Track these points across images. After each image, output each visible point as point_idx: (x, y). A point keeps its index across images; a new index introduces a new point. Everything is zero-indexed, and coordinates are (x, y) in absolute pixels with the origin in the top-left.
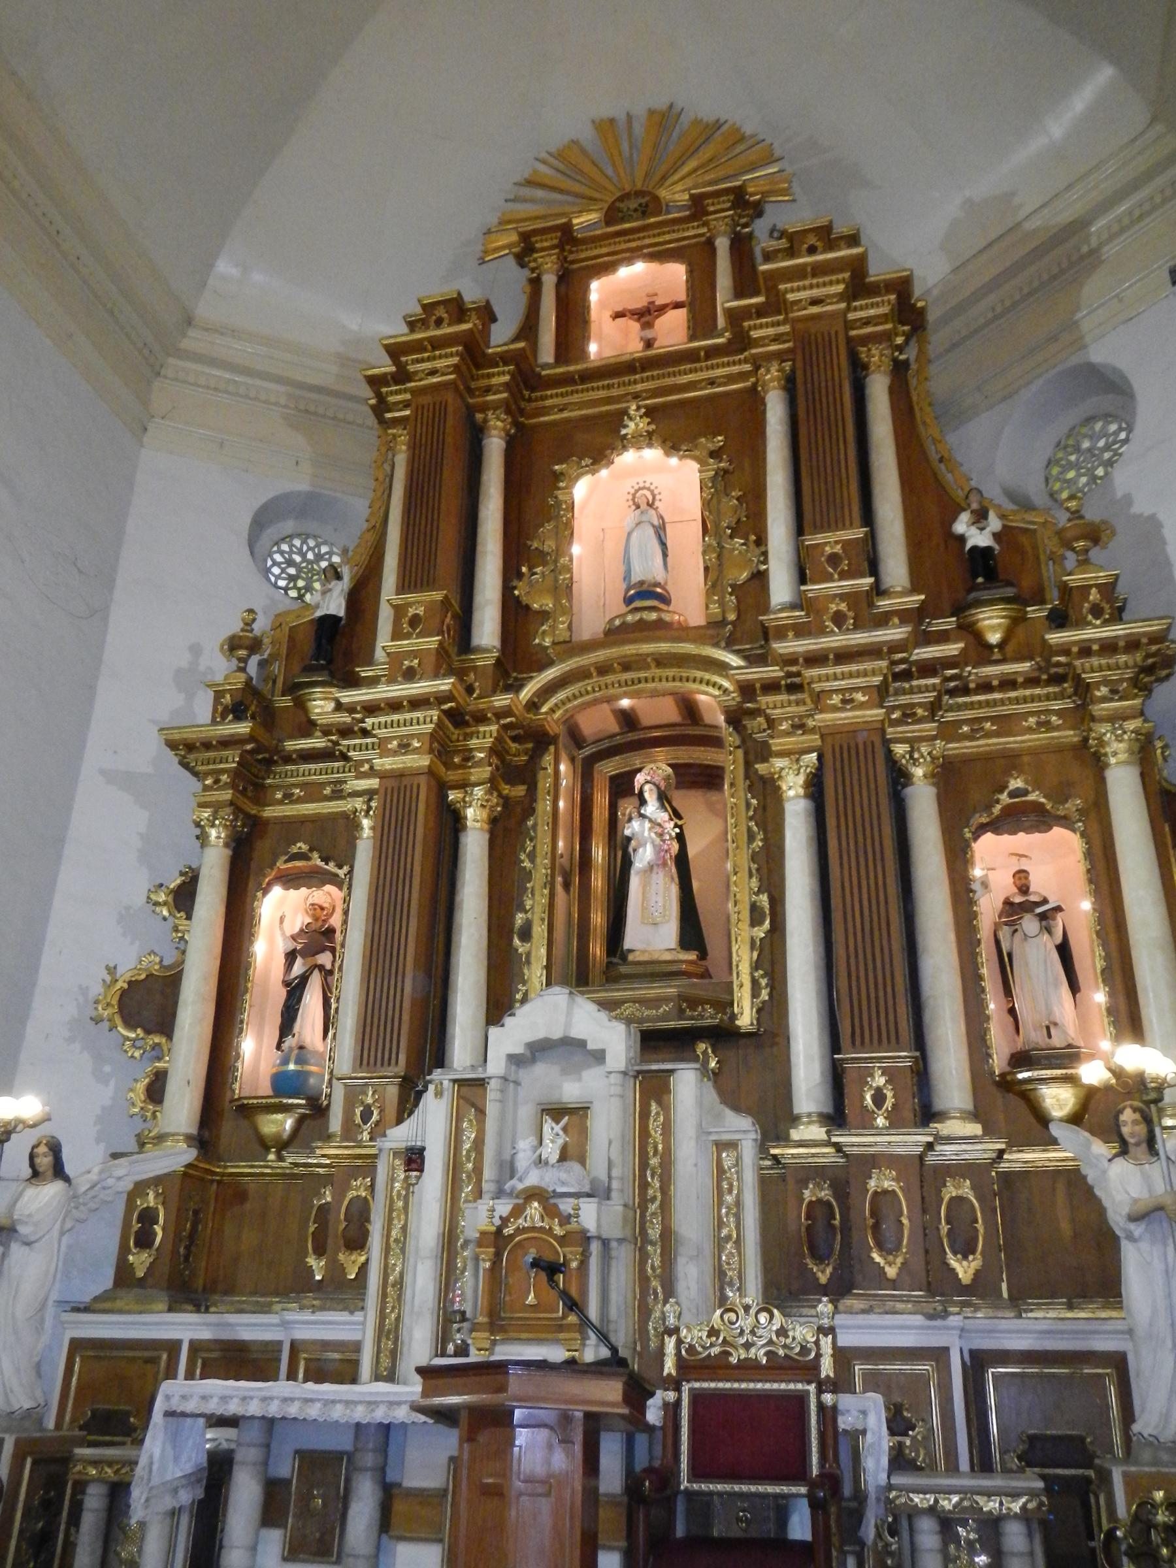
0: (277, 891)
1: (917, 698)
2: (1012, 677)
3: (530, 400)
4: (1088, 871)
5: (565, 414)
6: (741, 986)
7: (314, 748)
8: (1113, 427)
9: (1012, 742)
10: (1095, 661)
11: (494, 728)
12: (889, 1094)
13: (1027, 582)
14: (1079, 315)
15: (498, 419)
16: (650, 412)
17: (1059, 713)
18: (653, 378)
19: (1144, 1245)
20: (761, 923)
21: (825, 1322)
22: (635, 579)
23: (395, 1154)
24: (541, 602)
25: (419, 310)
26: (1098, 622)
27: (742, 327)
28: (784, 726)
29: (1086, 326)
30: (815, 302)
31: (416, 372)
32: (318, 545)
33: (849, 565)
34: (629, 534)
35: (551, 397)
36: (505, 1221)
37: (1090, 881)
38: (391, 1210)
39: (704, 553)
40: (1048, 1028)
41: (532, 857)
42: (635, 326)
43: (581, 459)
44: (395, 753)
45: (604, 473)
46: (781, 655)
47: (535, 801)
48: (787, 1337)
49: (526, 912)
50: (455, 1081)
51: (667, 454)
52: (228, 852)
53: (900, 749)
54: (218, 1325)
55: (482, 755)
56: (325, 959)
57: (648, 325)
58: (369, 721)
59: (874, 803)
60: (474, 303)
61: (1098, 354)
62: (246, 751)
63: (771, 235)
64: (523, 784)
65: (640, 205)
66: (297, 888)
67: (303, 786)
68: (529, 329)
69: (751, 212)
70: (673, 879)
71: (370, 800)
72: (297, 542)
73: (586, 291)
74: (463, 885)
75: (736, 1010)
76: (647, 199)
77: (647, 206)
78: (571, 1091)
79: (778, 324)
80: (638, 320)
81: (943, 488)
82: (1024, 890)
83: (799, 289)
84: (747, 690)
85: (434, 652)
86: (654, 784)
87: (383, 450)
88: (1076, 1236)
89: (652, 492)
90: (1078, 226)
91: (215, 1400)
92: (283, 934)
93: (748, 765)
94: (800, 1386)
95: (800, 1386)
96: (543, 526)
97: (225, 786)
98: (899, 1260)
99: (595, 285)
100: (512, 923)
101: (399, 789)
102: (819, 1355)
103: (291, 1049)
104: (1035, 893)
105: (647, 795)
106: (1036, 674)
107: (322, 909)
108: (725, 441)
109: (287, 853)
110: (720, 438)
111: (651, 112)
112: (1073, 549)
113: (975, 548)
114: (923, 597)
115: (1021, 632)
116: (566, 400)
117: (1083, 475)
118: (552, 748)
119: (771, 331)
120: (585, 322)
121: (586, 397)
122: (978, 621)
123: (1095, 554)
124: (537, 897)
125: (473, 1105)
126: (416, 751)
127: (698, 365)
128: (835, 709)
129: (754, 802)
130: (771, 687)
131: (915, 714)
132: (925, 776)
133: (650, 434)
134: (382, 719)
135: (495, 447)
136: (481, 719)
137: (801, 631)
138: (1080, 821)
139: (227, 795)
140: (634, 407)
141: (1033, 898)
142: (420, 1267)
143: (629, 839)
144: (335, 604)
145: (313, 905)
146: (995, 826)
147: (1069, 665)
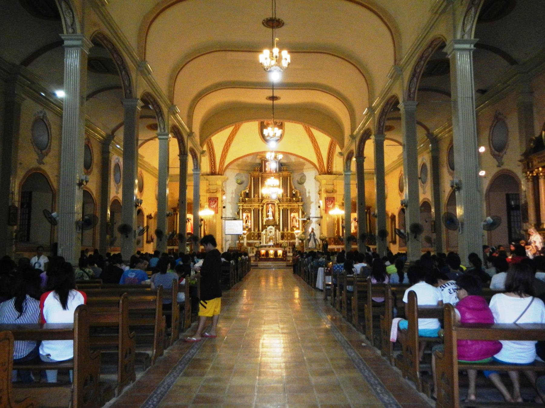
78: (271, 230)
144: (247, 192)
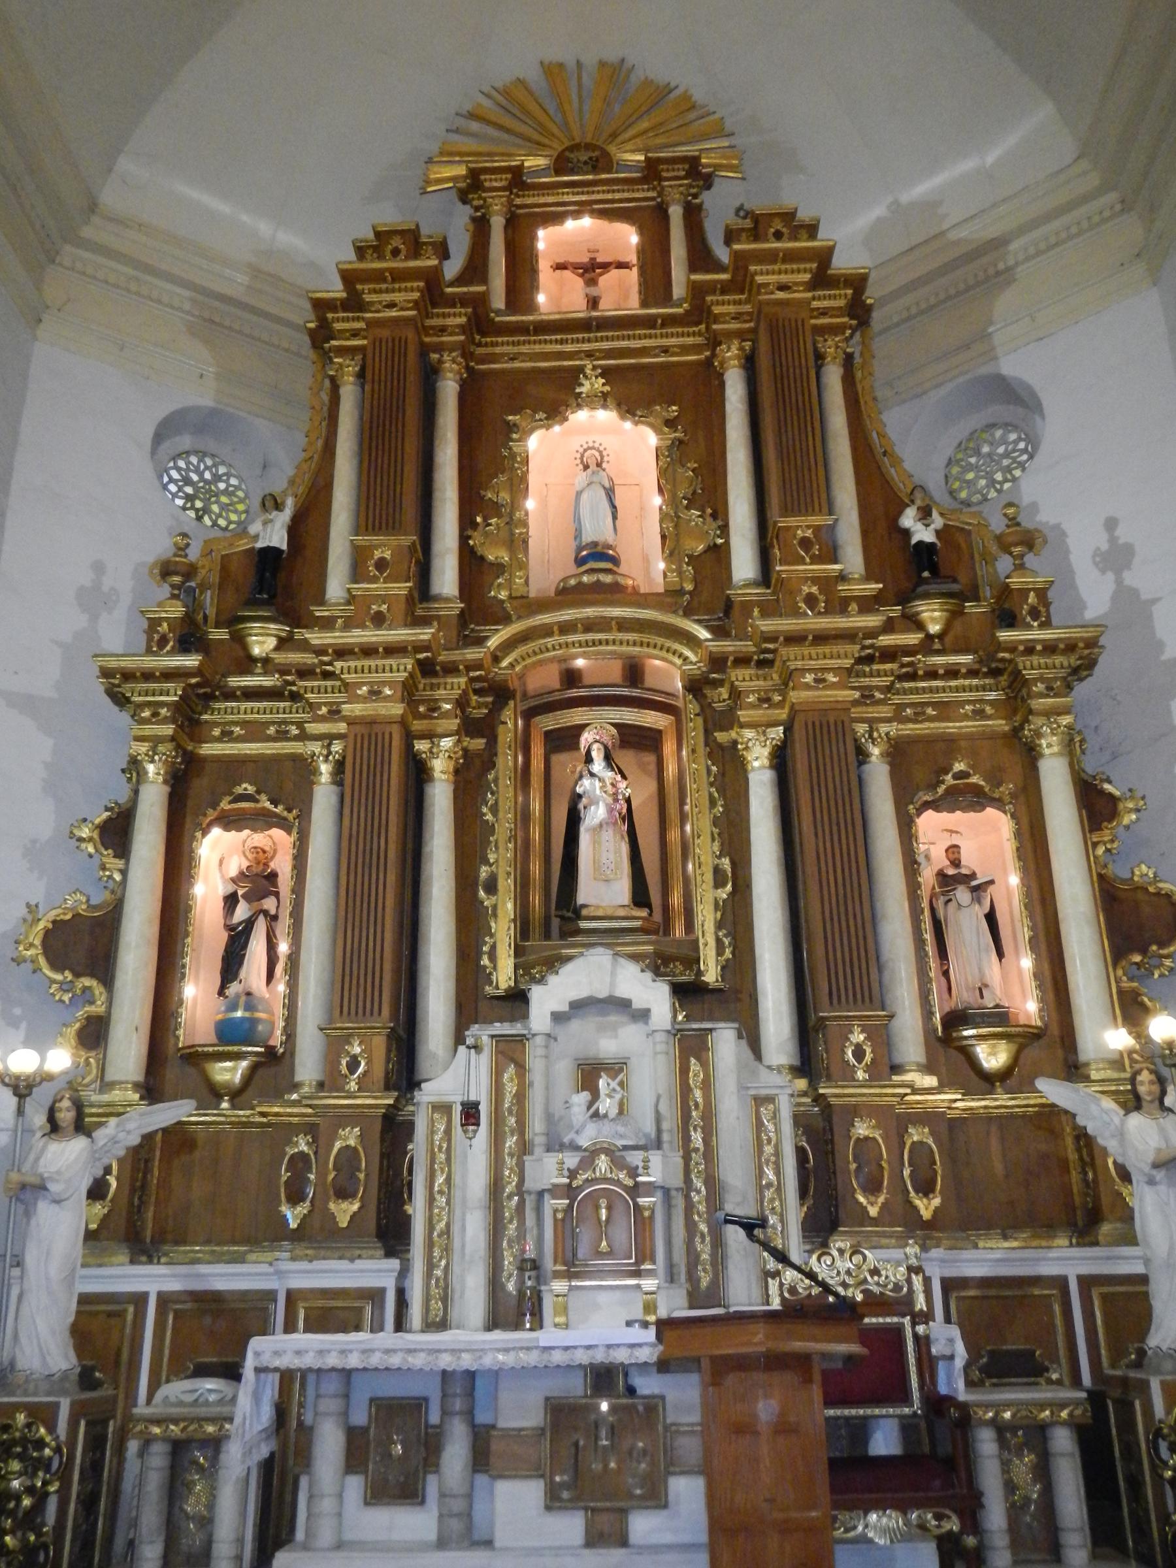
0: (216, 832)
1: (876, 681)
2: (957, 667)
3: (479, 345)
4: (1018, 849)
5: (517, 364)
6: (706, 945)
7: (261, 686)
8: (1013, 436)
9: (951, 727)
10: (1035, 660)
11: (463, 680)
12: (868, 1050)
13: (963, 578)
14: (990, 330)
15: (454, 361)
16: (606, 373)
17: (991, 703)
18: (607, 338)
19: (1162, 1188)
20: (724, 885)
21: (913, 1262)
22: (588, 537)
23: (433, 1107)
24: (494, 554)
25: (371, 236)
26: (1036, 624)
27: (704, 300)
28: (751, 699)
29: (998, 339)
30: (783, 287)
31: (372, 303)
32: (215, 465)
33: (819, 550)
34: (579, 494)
35: (503, 344)
36: (573, 1174)
37: (1020, 858)
38: (433, 1162)
39: (661, 521)
40: (980, 989)
41: (494, 810)
42: (579, 282)
43: (535, 412)
44: (364, 699)
45: (557, 429)
46: (762, 632)
47: (496, 755)
48: (880, 1275)
49: (491, 865)
50: (493, 1036)
51: (623, 417)
52: (166, 789)
53: (861, 728)
54: (186, 1276)
55: (448, 707)
56: (269, 904)
57: (591, 282)
58: (338, 665)
59: (845, 779)
60: (431, 237)
61: (1010, 366)
62: (190, 685)
63: (737, 214)
64: (483, 737)
65: (591, 158)
66: (239, 830)
67: (243, 724)
68: (476, 269)
69: (701, 183)
70: (623, 837)
71: (329, 745)
72: (194, 460)
73: (533, 238)
74: (432, 838)
75: (702, 968)
76: (597, 153)
77: (597, 160)
78: (608, 1047)
79: (740, 302)
80: (581, 275)
81: (887, 482)
82: (956, 863)
83: (768, 273)
84: (718, 662)
85: (403, 599)
86: (602, 743)
87: (319, 377)
88: (1007, 1176)
89: (600, 452)
90: (998, 244)
91: (311, 1354)
92: (223, 876)
93: (707, 732)
94: (895, 1320)
95: (895, 1320)
96: (497, 477)
97: (165, 721)
98: (881, 1199)
99: (541, 233)
100: (477, 877)
101: (370, 736)
102: (911, 1291)
103: (238, 996)
104: (966, 867)
105: (594, 754)
106: (976, 666)
107: (264, 852)
108: (680, 411)
109: (231, 794)
110: (674, 408)
111: (602, 64)
112: (1011, 554)
113: (920, 543)
114: (881, 586)
115: (958, 627)
116: (515, 349)
117: (982, 477)
118: (511, 703)
119: (732, 309)
120: (534, 271)
121: (537, 348)
122: (918, 613)
123: (1030, 560)
124: (501, 850)
125: (513, 1060)
126: (387, 698)
127: (653, 332)
128: (807, 687)
129: (714, 768)
130: (742, 661)
131: (873, 696)
132: (882, 754)
133: (605, 395)
134: (352, 664)
135: (449, 390)
136: (451, 669)
137: (768, 611)
138: (1011, 803)
139: (168, 730)
140: (590, 366)
141: (964, 871)
142: (469, 1217)
143: (580, 796)
145: (255, 848)
146: (935, 805)
147: (1010, 661)
